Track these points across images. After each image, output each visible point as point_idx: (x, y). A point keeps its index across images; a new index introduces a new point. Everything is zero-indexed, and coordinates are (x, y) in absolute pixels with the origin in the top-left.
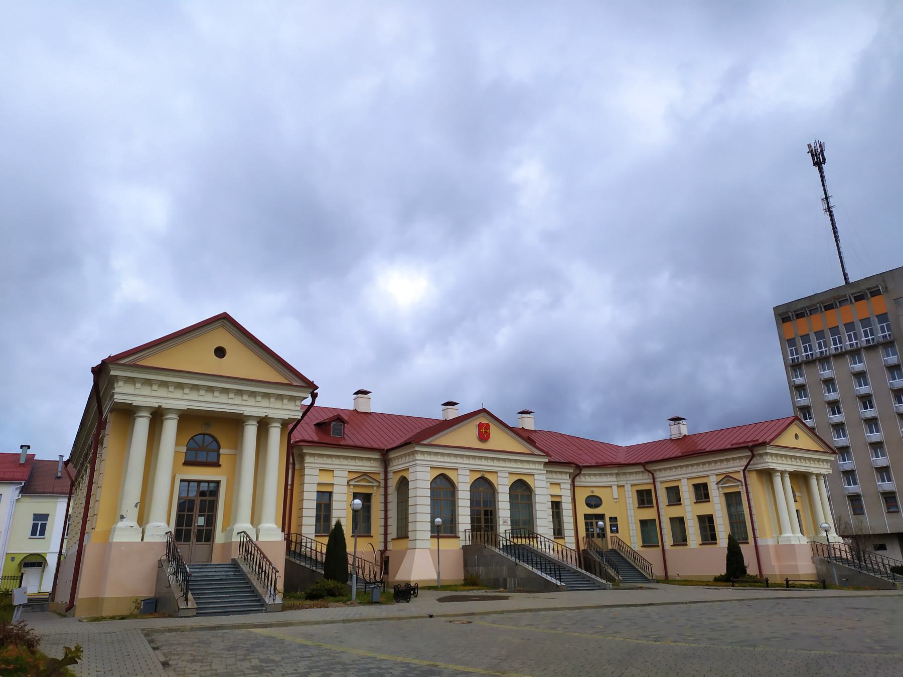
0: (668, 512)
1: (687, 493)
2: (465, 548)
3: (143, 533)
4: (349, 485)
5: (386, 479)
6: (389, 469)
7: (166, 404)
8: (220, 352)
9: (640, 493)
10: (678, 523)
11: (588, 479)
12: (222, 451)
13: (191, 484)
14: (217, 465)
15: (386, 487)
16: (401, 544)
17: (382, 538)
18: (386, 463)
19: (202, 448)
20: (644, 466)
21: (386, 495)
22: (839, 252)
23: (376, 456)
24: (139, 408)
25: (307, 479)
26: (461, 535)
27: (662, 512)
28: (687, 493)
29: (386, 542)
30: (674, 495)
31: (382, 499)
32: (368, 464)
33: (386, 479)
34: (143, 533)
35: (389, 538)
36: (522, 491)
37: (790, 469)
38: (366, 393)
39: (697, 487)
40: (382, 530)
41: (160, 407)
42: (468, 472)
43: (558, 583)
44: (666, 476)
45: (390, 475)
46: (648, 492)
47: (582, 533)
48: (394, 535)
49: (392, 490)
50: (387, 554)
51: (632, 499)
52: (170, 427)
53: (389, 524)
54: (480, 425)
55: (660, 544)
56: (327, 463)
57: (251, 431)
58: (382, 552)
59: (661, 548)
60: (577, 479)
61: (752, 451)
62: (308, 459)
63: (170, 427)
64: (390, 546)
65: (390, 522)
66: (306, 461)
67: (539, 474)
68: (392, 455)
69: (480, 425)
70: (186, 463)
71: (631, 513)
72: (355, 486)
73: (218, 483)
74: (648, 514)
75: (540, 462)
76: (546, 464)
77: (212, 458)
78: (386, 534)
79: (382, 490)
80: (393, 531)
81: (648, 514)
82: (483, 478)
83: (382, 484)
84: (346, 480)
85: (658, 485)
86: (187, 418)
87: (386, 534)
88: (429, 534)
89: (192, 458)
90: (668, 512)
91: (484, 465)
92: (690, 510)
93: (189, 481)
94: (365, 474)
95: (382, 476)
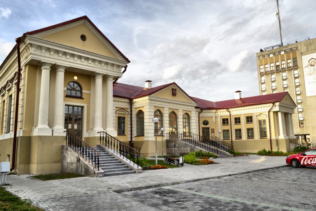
0: (235, 127)
1: (243, 120)
2: (167, 141)
3: (53, 131)
4: (116, 113)
6: (133, 107)
7: (59, 63)
8: (83, 38)
9: (224, 120)
10: (239, 131)
11: (206, 114)
12: (84, 91)
13: (70, 107)
14: (81, 98)
15: (131, 115)
16: (140, 139)
17: (130, 136)
19: (73, 89)
20: (227, 109)
21: (131, 118)
22: (281, 34)
23: (127, 100)
24: (44, 63)
26: (165, 135)
27: (232, 127)
28: (243, 120)
29: (131, 138)
30: (238, 120)
31: (129, 119)
32: (123, 104)
33: (131, 111)
34: (53, 131)
35: (133, 136)
36: (187, 116)
37: (284, 111)
39: (247, 118)
40: (129, 133)
41: (55, 64)
42: (168, 109)
43: (217, 155)
44: (236, 112)
45: (133, 109)
46: (227, 119)
47: (201, 135)
48: (136, 135)
49: (134, 116)
51: (220, 122)
52: (61, 75)
53: (133, 130)
54: (173, 89)
55: (230, 138)
57: (99, 81)
59: (231, 140)
60: (200, 114)
61: (273, 104)
63: (61, 75)
64: (134, 139)
65: (133, 129)
67: (193, 111)
69: (173, 89)
70: (67, 96)
71: (219, 127)
72: (118, 113)
73: (82, 107)
74: (227, 127)
75: (194, 106)
76: (196, 107)
77: (79, 94)
78: (131, 134)
79: (129, 116)
80: (135, 133)
81: (227, 127)
82: (173, 112)
83: (130, 113)
84: (115, 111)
85: (232, 117)
86: (70, 72)
87: (131, 134)
88: (153, 135)
90: (235, 127)
91: (174, 107)
92: (244, 126)
93: (69, 106)
94: (123, 108)
95: (129, 110)
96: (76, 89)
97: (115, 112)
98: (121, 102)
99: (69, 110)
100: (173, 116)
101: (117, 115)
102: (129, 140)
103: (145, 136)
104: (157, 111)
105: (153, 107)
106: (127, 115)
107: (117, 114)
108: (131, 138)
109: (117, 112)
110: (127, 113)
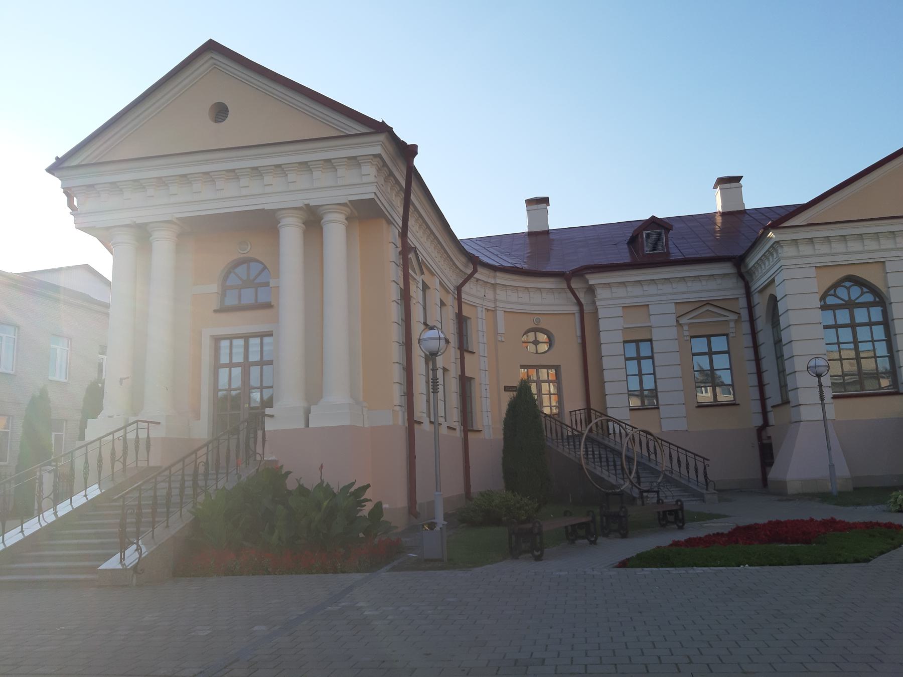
4: (679, 325)
5: (750, 308)
6: (753, 289)
15: (752, 320)
17: (757, 407)
18: (744, 277)
21: (754, 334)
23: (727, 268)
25: (603, 325)
29: (765, 413)
33: (750, 308)
35: (770, 403)
38: (738, 179)
50: (770, 431)
56: (634, 295)
58: (761, 430)
62: (601, 293)
65: (766, 378)
66: (599, 297)
68: (752, 261)
78: (763, 399)
79: (746, 327)
84: (674, 316)
87: (763, 399)
89: (231, 301)
94: (708, 303)
95: (743, 302)
96: (257, 281)
97: (675, 324)
98: (624, 284)
99: (234, 351)
100: (863, 299)
101: (686, 333)
102: (759, 422)
103: (792, 404)
104: (848, 284)
105: (812, 272)
106: (732, 324)
107: (686, 328)
108: (765, 413)
109: (682, 321)
110: (733, 317)
